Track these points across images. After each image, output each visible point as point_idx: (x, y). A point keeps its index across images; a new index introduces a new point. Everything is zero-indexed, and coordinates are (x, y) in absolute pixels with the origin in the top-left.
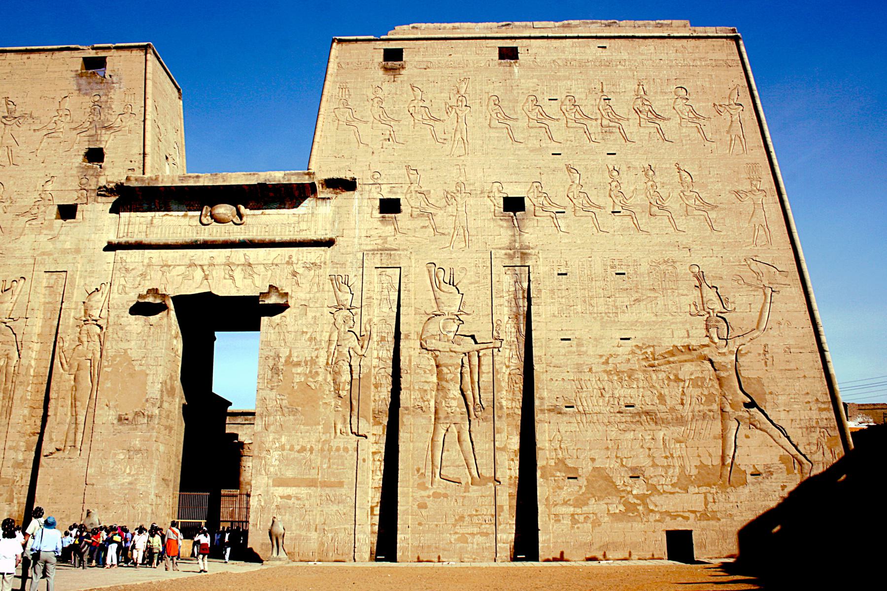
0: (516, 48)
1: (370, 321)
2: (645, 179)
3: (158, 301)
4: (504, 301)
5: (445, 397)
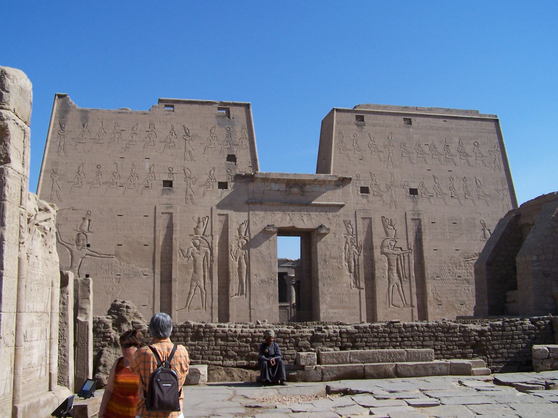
0: (410, 119)
1: (361, 240)
2: (463, 182)
3: (275, 230)
4: (411, 234)
5: (392, 273)
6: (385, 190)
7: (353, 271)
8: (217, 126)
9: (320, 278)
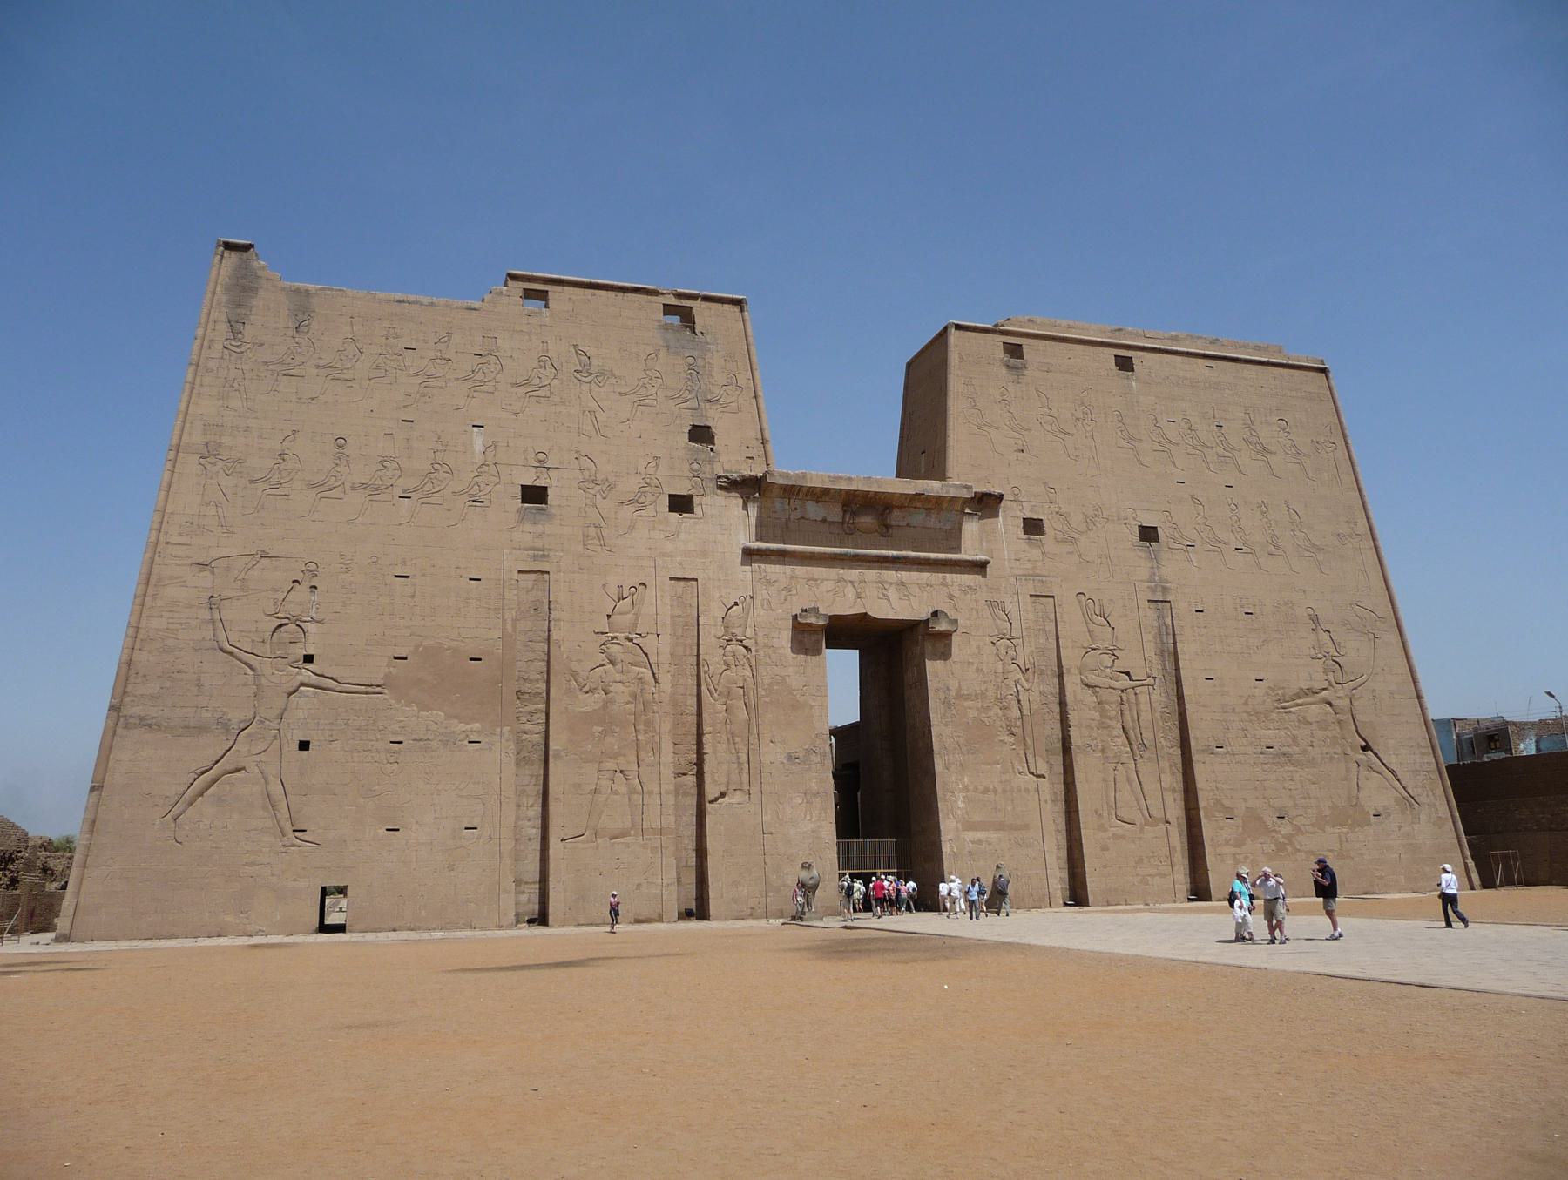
3: (821, 622)
6: (1083, 527)
7: (1015, 730)
8: (663, 351)
9: (935, 748)
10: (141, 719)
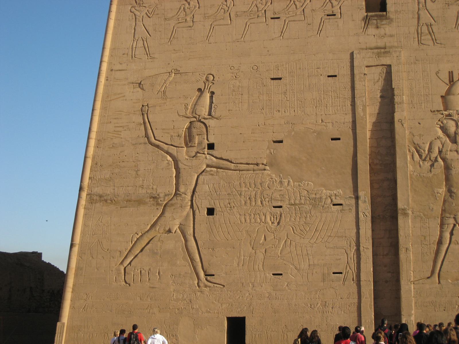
10: (101, 196)
